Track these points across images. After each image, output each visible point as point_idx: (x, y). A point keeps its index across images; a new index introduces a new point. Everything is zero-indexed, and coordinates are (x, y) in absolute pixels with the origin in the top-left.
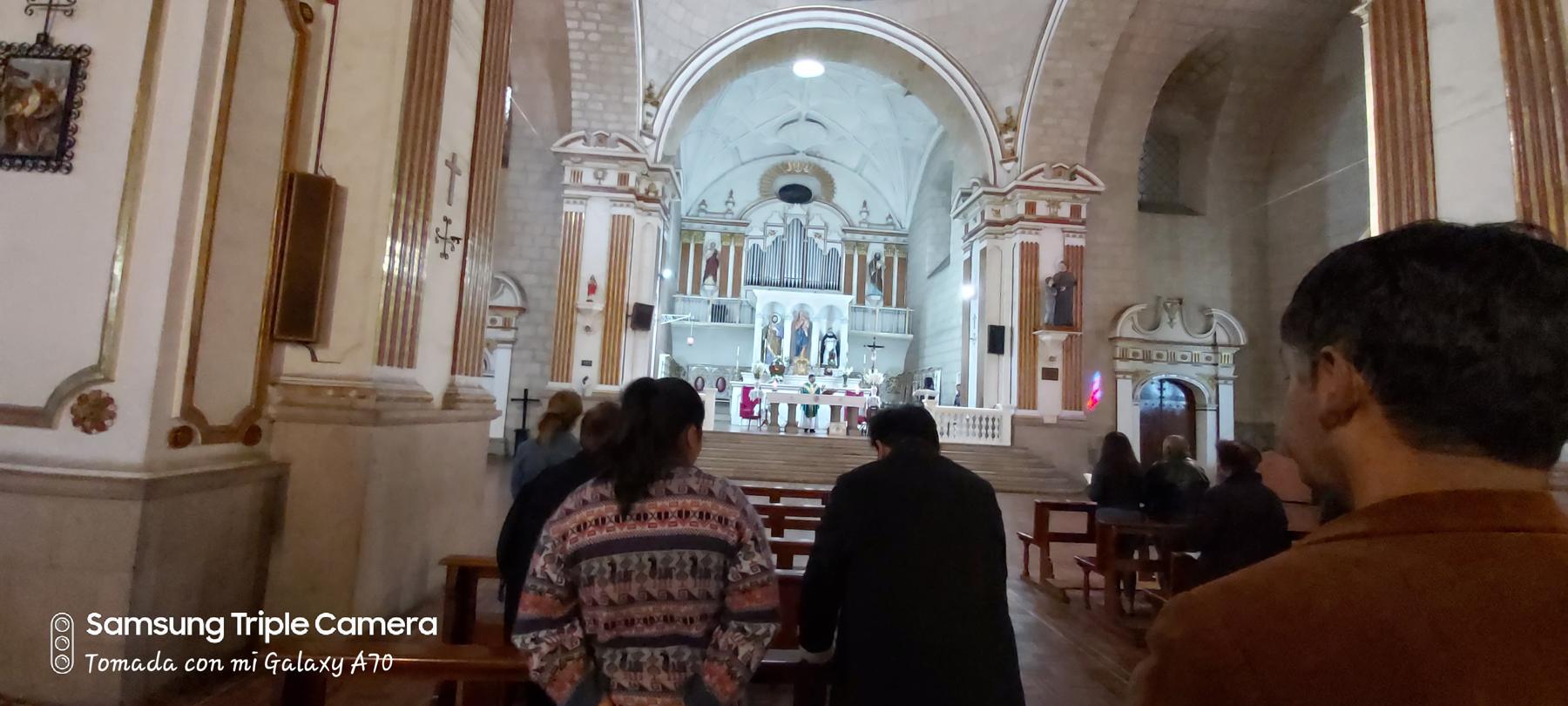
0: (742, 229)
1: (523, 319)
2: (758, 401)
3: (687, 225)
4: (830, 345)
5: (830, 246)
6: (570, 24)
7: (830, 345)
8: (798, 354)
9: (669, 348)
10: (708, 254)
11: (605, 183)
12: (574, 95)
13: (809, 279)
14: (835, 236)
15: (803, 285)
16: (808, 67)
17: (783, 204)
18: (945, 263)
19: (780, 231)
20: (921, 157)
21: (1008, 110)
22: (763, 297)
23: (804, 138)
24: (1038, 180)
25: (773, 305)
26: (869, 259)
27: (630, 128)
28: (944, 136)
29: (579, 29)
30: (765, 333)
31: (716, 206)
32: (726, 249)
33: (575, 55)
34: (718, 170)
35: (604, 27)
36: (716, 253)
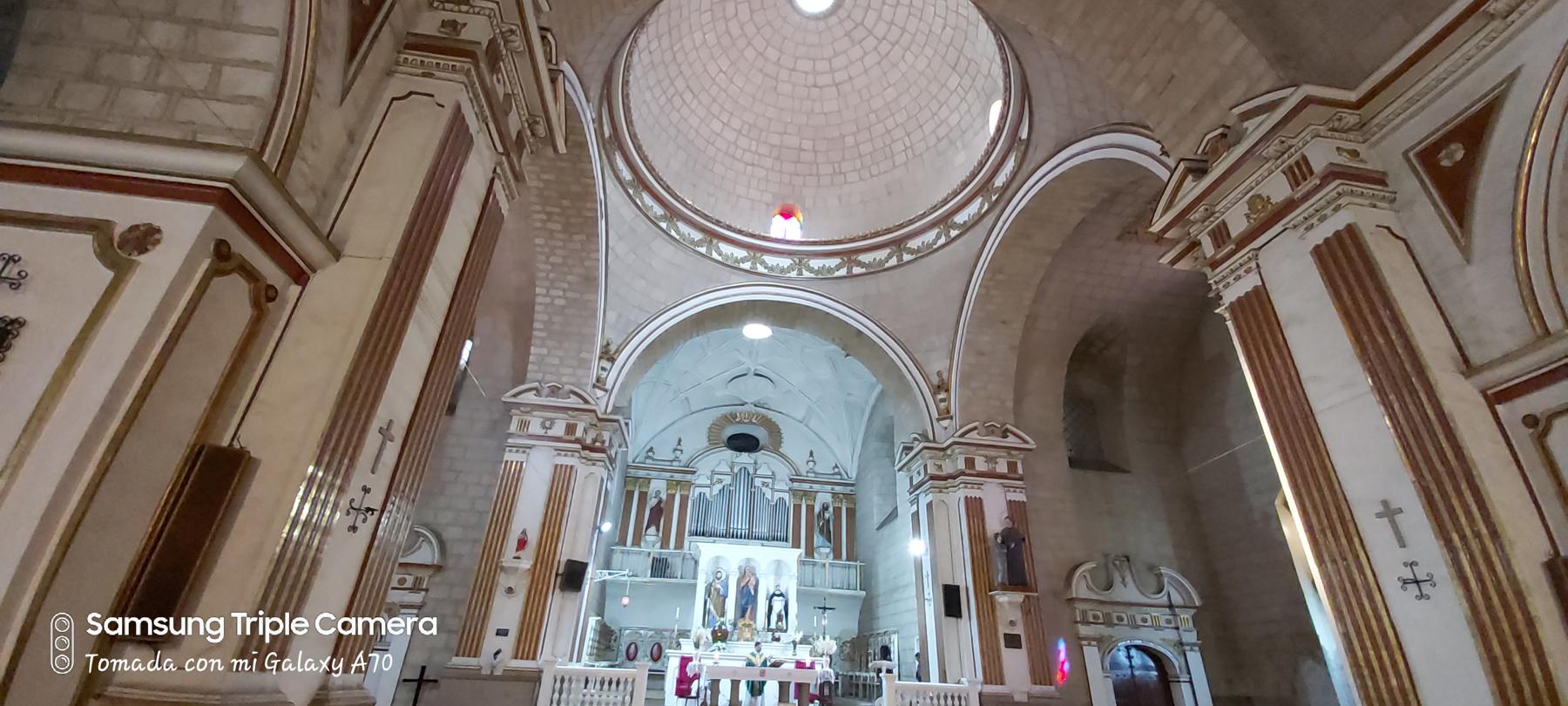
0: (689, 477)
1: (437, 579)
2: (696, 676)
3: (632, 472)
4: (778, 605)
5: (777, 495)
6: (538, 290)
7: (778, 605)
8: (743, 616)
9: (600, 613)
10: (652, 502)
11: (550, 433)
12: (533, 350)
15: (750, 537)
16: (756, 331)
17: (730, 452)
18: (893, 515)
19: (727, 480)
20: (863, 411)
21: (939, 374)
22: (708, 552)
23: (753, 391)
24: (974, 437)
25: (717, 559)
26: (817, 509)
27: (584, 381)
28: (882, 393)
29: (547, 295)
30: (708, 592)
31: (664, 453)
32: (671, 497)
33: (540, 317)
34: (665, 421)
35: (569, 294)
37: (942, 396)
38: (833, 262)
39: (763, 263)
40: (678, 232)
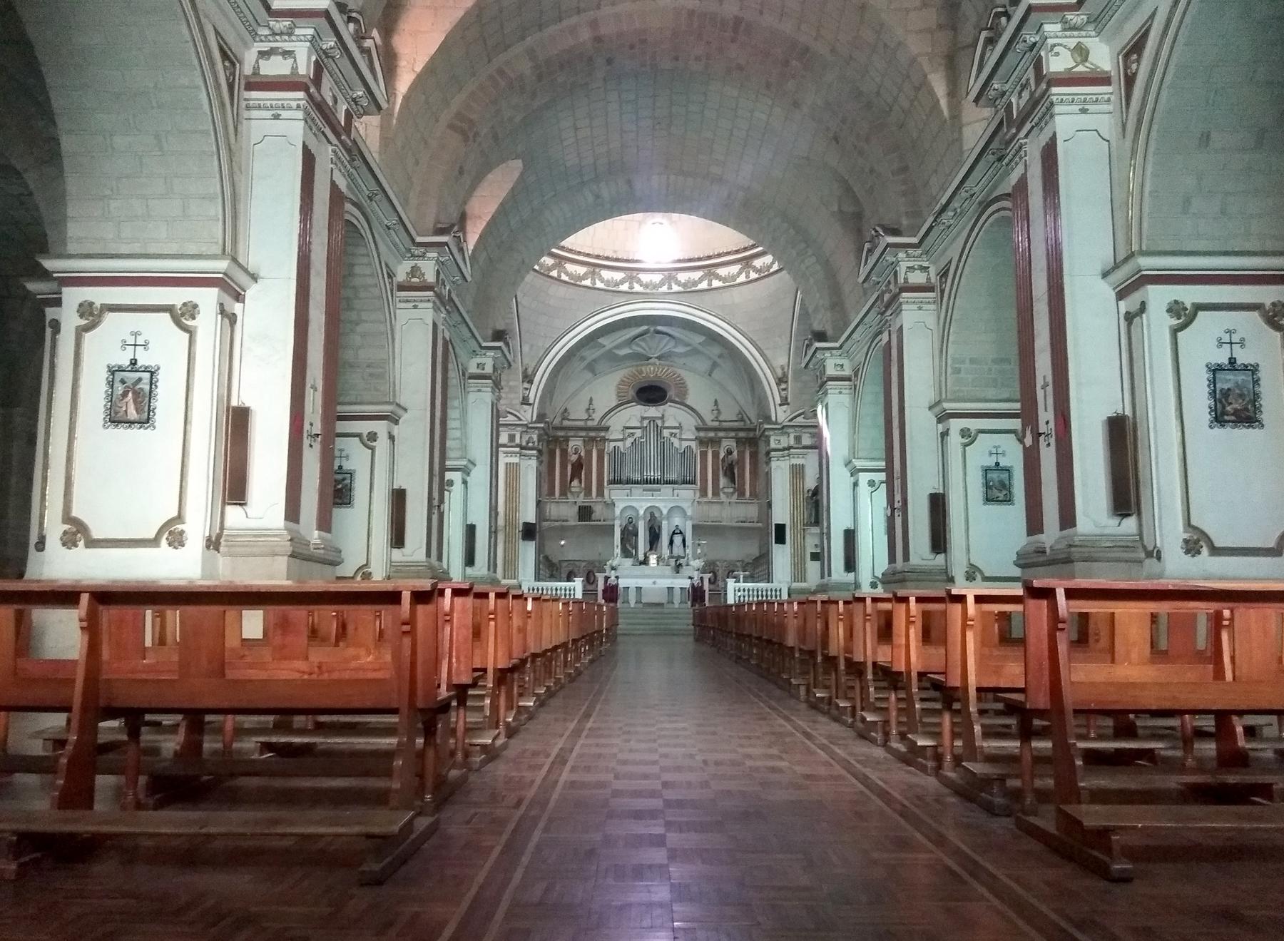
4: (678, 539)
5: (685, 444)
10: (574, 458)
13: (668, 477)
14: (689, 434)
26: (722, 455)
32: (589, 453)
36: (580, 457)
37: (783, 386)
38: (697, 275)
39: (639, 282)
40: (567, 274)
